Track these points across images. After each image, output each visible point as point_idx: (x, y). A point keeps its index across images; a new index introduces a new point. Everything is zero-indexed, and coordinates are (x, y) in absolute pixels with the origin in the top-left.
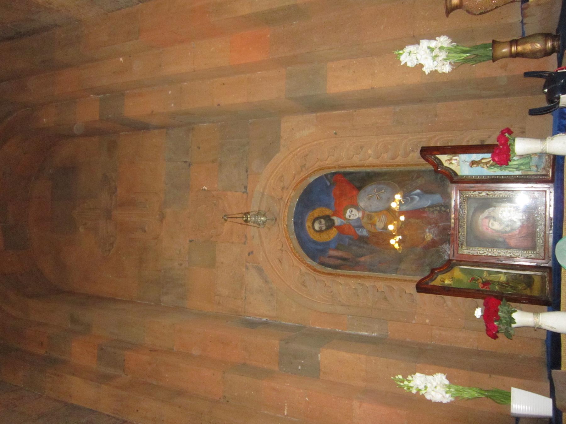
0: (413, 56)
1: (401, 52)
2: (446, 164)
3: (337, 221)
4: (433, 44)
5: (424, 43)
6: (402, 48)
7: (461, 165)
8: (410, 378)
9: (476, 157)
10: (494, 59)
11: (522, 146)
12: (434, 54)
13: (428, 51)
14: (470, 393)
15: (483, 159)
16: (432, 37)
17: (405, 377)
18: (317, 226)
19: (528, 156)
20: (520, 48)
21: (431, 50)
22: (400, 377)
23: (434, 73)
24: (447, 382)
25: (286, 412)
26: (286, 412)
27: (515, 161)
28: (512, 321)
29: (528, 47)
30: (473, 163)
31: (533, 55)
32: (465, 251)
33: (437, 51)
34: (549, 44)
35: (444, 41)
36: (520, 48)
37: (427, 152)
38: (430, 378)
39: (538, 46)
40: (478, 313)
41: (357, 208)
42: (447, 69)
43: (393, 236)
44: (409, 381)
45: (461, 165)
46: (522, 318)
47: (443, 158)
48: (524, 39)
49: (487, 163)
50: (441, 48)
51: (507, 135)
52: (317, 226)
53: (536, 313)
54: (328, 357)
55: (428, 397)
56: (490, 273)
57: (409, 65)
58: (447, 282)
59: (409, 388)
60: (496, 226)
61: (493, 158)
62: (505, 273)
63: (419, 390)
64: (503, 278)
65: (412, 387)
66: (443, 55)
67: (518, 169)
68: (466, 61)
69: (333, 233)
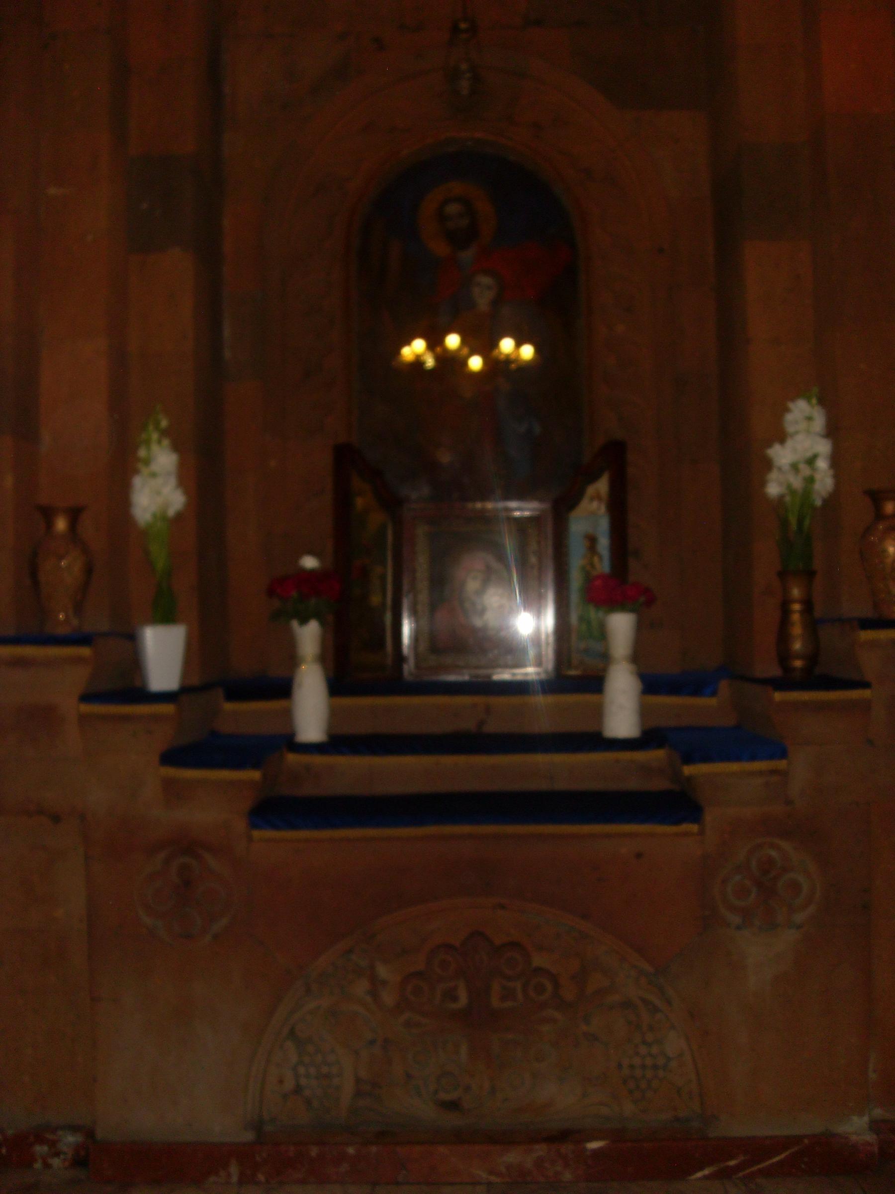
0: (803, 425)
1: (814, 401)
2: (591, 490)
3: (467, 255)
4: (822, 464)
5: (823, 447)
6: (822, 402)
7: (591, 517)
8: (166, 442)
9: (604, 543)
10: (783, 575)
11: (621, 625)
12: (802, 466)
13: (809, 454)
14: (160, 557)
15: (600, 558)
16: (836, 461)
17: (165, 433)
18: (453, 209)
19: (602, 634)
20: (796, 617)
21: (811, 461)
22: (164, 423)
23: (768, 465)
24: (171, 512)
25: (52, 191)
26: (52, 191)
27: (593, 614)
28: (304, 621)
29: (797, 630)
30: (592, 540)
31: (783, 637)
32: (421, 530)
33: (806, 471)
34: (798, 663)
35: (824, 481)
36: (796, 617)
37: (614, 457)
38: (173, 481)
39: (797, 646)
40: (309, 562)
41: (496, 303)
42: (773, 489)
43: (431, 347)
44: (159, 442)
45: (591, 517)
46: (309, 636)
47: (602, 486)
48: (812, 625)
49: (592, 565)
50: (810, 480)
51: (642, 599)
52: (453, 209)
53: (322, 659)
54: (177, 265)
55: (137, 481)
56: (383, 579)
57: (789, 417)
58: (359, 503)
59: (148, 443)
60: (472, 585)
61: (601, 577)
62: (383, 604)
63: (147, 462)
64: (375, 600)
65: (149, 449)
66: (797, 483)
67: (581, 619)
68: (784, 523)
69: (440, 248)
